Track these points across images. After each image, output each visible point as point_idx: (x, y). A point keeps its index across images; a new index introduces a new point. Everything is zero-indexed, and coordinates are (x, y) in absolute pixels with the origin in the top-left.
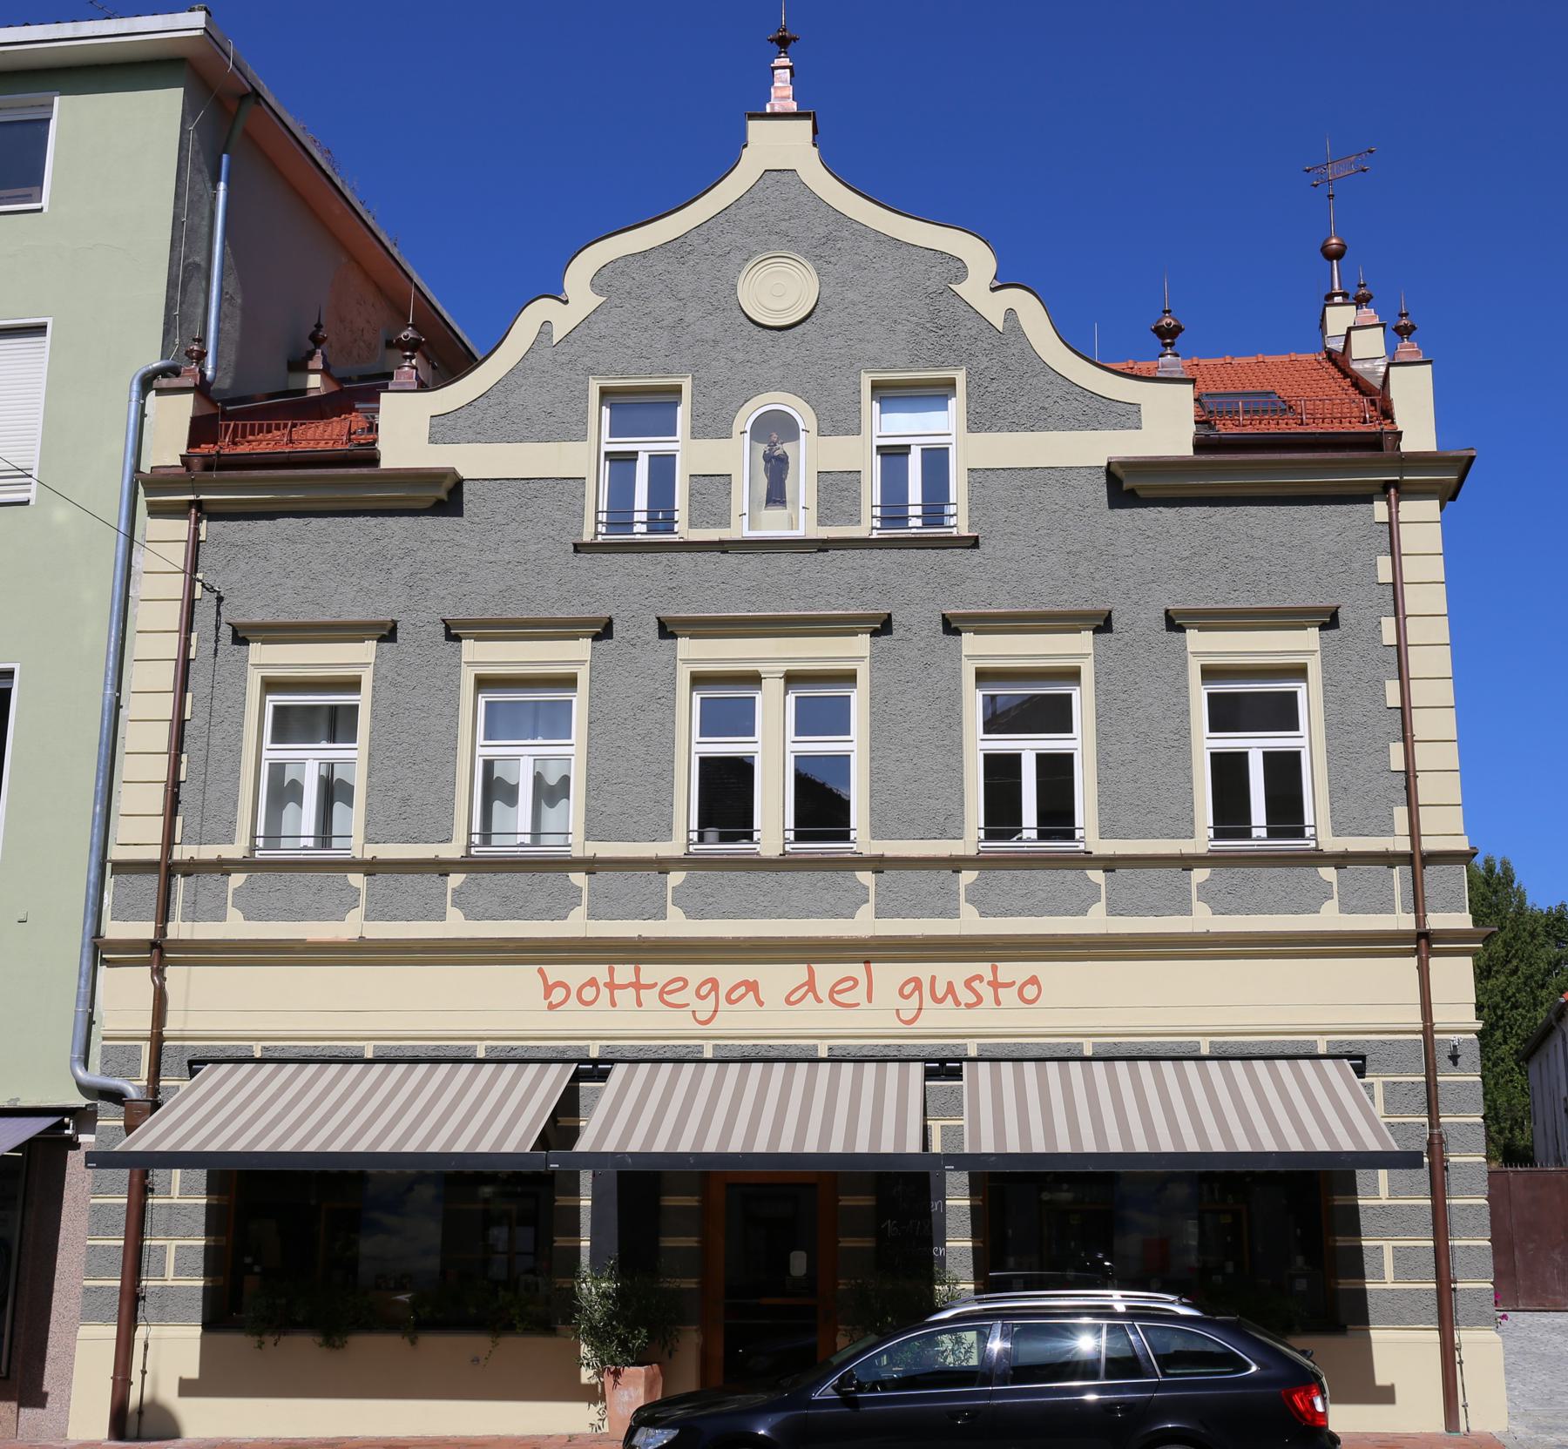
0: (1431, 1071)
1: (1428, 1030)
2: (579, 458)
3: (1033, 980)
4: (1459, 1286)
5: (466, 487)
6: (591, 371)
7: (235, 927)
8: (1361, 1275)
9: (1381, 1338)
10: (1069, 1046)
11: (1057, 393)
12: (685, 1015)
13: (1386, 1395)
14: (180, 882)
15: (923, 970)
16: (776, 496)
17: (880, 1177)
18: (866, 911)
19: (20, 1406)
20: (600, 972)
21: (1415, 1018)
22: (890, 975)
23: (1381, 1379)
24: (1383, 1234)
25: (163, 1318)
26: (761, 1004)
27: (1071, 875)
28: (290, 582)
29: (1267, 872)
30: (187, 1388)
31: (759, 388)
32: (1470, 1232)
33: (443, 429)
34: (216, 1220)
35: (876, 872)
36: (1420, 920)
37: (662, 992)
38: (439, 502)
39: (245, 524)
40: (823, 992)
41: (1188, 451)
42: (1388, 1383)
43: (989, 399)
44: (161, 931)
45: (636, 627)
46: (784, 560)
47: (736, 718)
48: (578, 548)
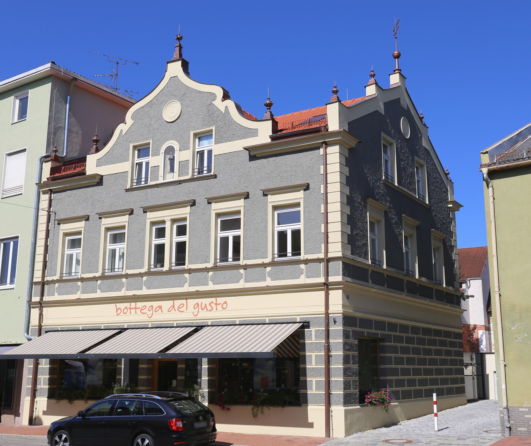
0: (327, 325)
1: (327, 314)
2: (126, 167)
3: (226, 303)
4: (333, 392)
5: (104, 177)
6: (130, 142)
7: (56, 297)
8: (306, 388)
9: (311, 408)
10: (233, 321)
11: (238, 129)
12: (146, 315)
13: (311, 425)
14: (46, 287)
15: (199, 301)
16: (172, 170)
17: (186, 359)
18: (303, 277)
19: (15, 416)
20: (127, 305)
21: (323, 310)
22: (192, 302)
23: (310, 421)
24: (313, 376)
25: (41, 396)
26: (162, 312)
27: (235, 271)
28: (69, 208)
29: (286, 267)
30: (45, 413)
31: (167, 140)
32: (337, 376)
33: (100, 163)
34: (52, 371)
35: (245, 269)
36: (327, 279)
37: (141, 310)
38: (98, 183)
39: (60, 194)
40: (176, 309)
41: (269, 141)
42: (311, 422)
43: (221, 134)
44: (41, 299)
45: (201, 201)
46: (171, 188)
47: (161, 233)
48: (127, 190)
